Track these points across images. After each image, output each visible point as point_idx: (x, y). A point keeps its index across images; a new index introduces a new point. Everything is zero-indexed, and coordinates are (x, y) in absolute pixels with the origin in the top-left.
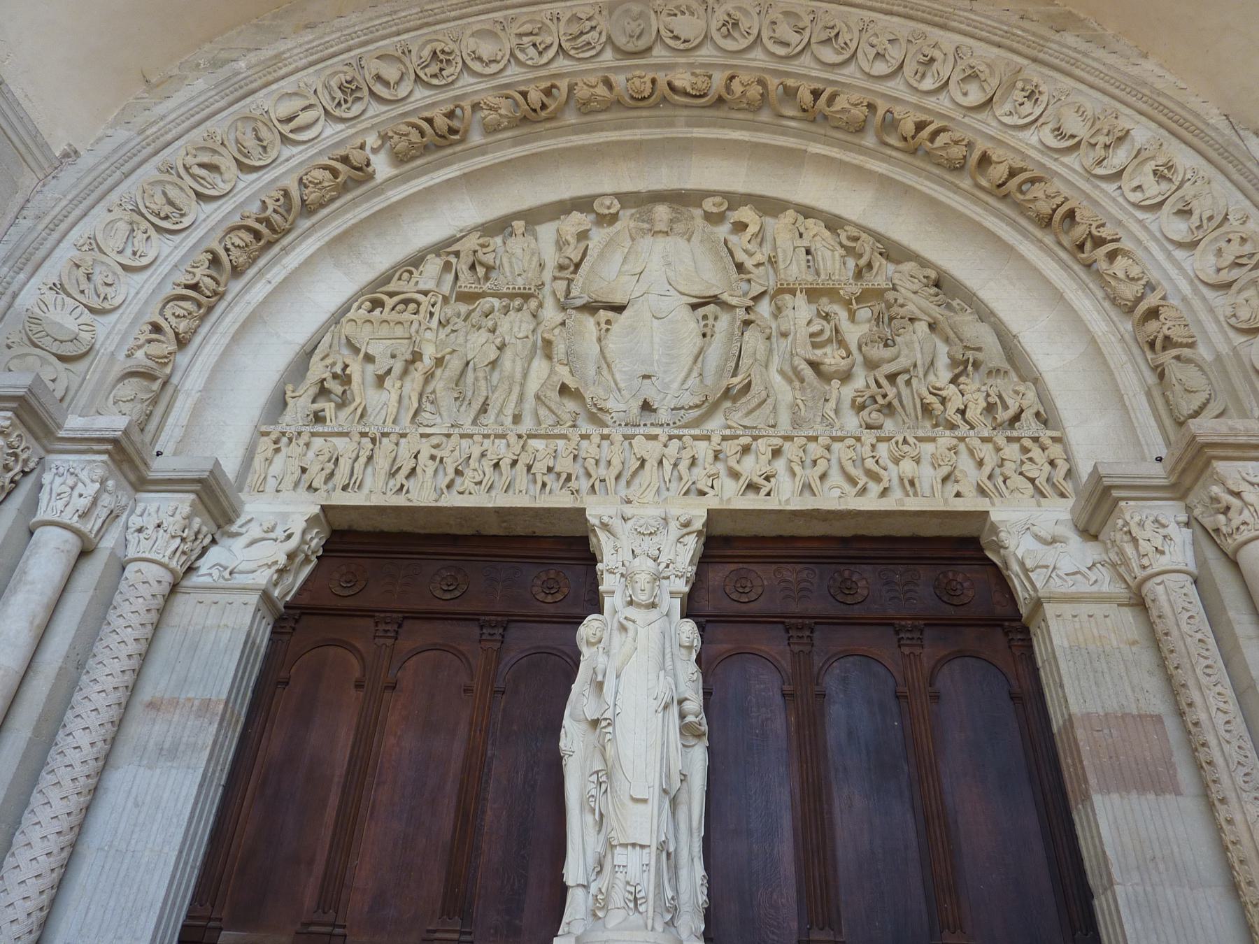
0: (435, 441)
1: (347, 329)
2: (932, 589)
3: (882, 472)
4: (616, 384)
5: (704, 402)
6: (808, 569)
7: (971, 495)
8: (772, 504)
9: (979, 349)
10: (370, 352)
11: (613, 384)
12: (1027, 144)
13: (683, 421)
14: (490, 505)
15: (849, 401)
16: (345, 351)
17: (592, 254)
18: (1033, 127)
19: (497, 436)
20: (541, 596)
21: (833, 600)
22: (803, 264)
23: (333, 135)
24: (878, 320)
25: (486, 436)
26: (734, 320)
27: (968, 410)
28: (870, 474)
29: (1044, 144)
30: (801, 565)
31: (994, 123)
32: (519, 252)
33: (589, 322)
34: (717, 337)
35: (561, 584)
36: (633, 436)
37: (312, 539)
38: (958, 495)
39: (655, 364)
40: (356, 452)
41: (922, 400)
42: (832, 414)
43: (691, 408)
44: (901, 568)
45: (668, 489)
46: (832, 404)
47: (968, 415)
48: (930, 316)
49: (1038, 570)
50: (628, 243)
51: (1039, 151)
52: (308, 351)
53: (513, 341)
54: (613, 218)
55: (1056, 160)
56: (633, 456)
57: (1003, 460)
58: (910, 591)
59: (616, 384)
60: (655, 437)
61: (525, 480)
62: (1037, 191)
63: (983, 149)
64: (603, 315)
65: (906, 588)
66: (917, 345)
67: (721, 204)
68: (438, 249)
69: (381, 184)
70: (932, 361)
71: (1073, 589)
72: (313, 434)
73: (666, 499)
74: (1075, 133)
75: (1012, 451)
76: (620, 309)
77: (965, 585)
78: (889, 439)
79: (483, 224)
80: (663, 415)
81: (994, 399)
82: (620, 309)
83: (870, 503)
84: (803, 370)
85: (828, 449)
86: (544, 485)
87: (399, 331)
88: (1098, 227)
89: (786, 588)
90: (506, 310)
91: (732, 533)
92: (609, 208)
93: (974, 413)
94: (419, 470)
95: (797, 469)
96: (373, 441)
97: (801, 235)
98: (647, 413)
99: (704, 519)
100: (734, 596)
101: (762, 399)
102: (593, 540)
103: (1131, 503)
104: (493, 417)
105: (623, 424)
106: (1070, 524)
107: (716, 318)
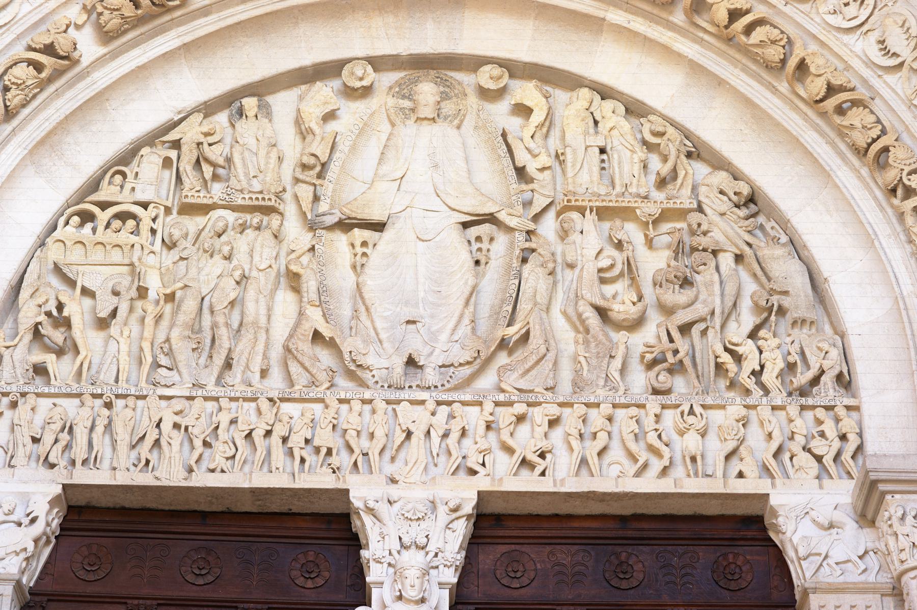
0: (178, 405)
1: (54, 253)
2: (709, 572)
3: (664, 449)
4: (377, 334)
5: (475, 358)
6: (584, 551)
7: (753, 475)
8: (545, 486)
9: (786, 293)
10: (87, 285)
11: (372, 333)
12: (851, 51)
13: (454, 382)
14: (246, 485)
15: (638, 355)
16: (55, 281)
17: (343, 145)
18: (859, 32)
19: (246, 399)
20: (300, 581)
21: (607, 585)
22: (596, 169)
23: (30, 12)
24: (678, 250)
25: (232, 399)
26: (512, 245)
27: (765, 370)
28: (652, 449)
29: (866, 56)
30: (576, 547)
31: (818, 20)
32: (252, 142)
33: (341, 240)
34: (492, 263)
35: (321, 567)
36: (398, 402)
37: (53, 519)
38: (741, 475)
39: (421, 305)
40: (91, 419)
41: (717, 357)
42: (617, 375)
43: (461, 365)
44: (681, 549)
45: (436, 465)
46: (617, 363)
47: (765, 378)
48: (737, 247)
49: (811, 558)
50: (386, 127)
51: (864, 62)
52: (14, 284)
53: (254, 273)
54: (366, 91)
55: (879, 76)
56: (398, 428)
57: (792, 432)
58: (687, 574)
59: (377, 334)
60: (422, 402)
61: (281, 456)
62: (856, 117)
63: (802, 55)
64: (359, 234)
65: (683, 572)
66: (717, 288)
67: (500, 78)
68: (151, 139)
69: (87, 67)
70: (735, 305)
71: (841, 579)
72: (38, 395)
73: (434, 478)
74: (898, 53)
75: (803, 424)
76: (379, 227)
77: (744, 569)
78: (677, 406)
79: (205, 102)
80: (431, 376)
81: (795, 358)
82: (379, 227)
83: (649, 484)
84: (587, 318)
85: (610, 419)
86: (303, 460)
87: (116, 256)
88: (910, 174)
89: (560, 573)
90: (243, 228)
91: (504, 512)
92: (361, 79)
93: (769, 377)
94: (163, 442)
95: (575, 443)
96: (109, 405)
97: (596, 123)
98: (412, 370)
99: (474, 502)
100: (504, 581)
101: (541, 355)
102: (356, 523)
103: (897, 496)
104: (239, 376)
105: (386, 385)
106: (850, 510)
107: (492, 239)
